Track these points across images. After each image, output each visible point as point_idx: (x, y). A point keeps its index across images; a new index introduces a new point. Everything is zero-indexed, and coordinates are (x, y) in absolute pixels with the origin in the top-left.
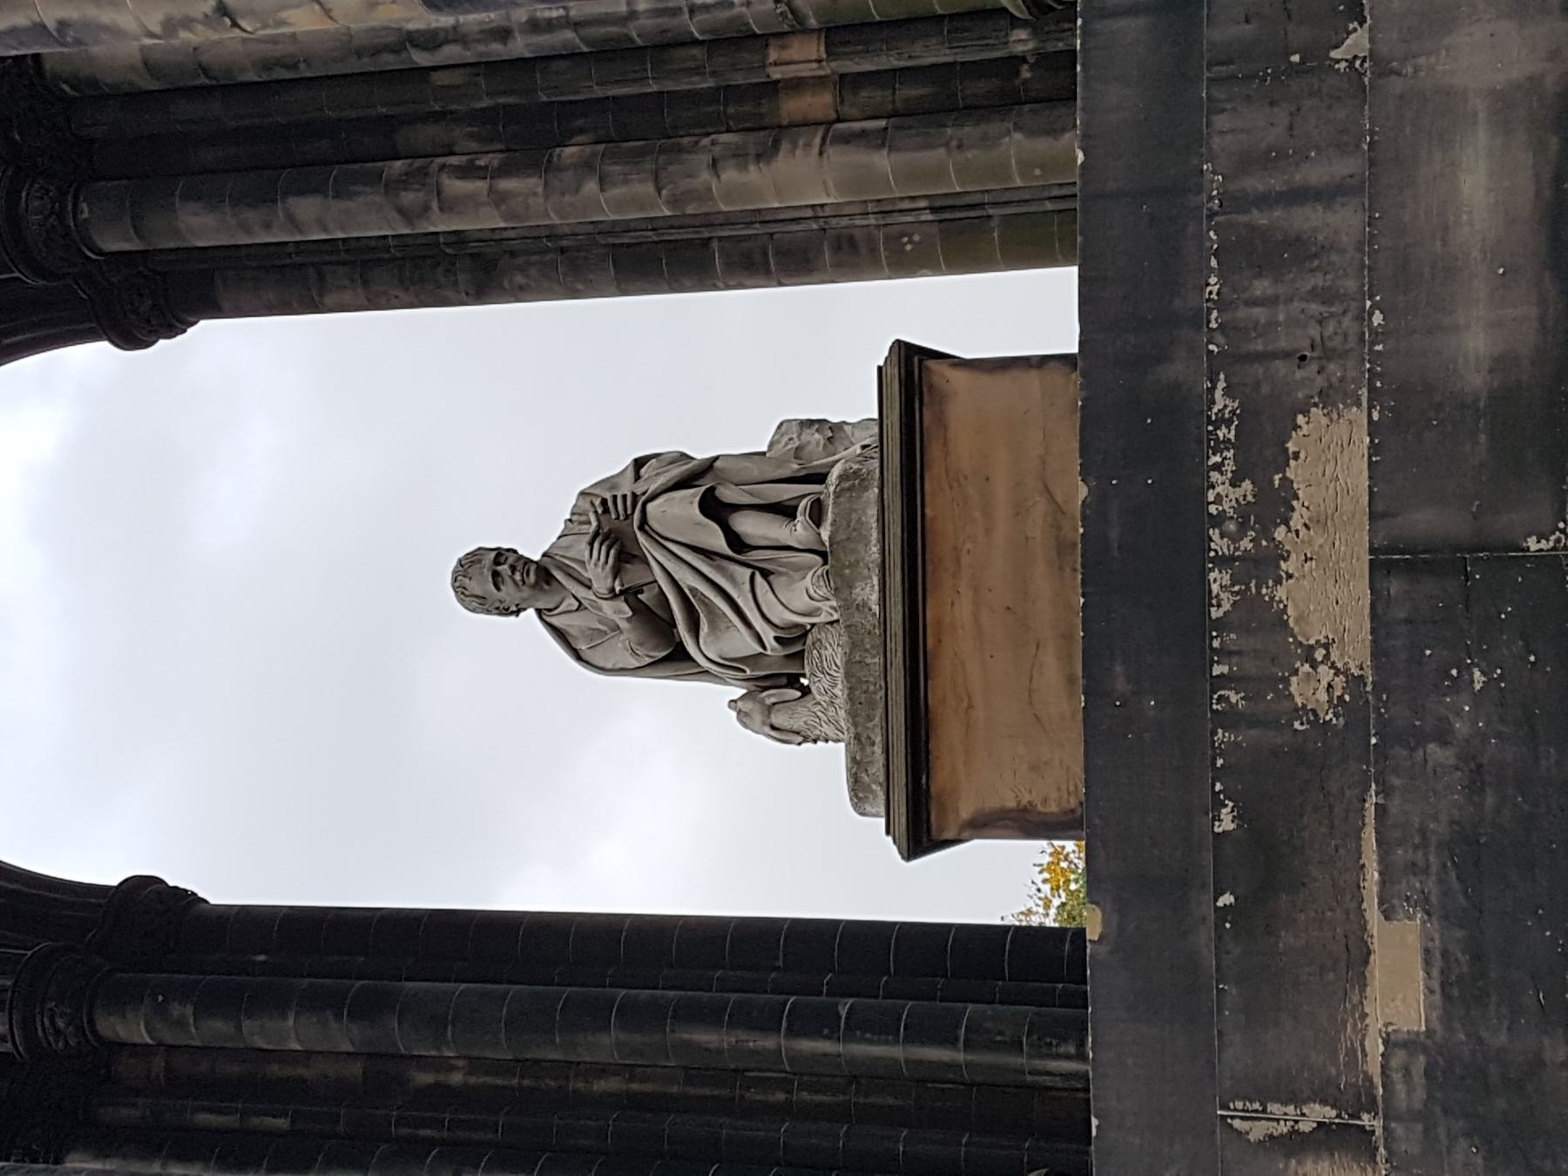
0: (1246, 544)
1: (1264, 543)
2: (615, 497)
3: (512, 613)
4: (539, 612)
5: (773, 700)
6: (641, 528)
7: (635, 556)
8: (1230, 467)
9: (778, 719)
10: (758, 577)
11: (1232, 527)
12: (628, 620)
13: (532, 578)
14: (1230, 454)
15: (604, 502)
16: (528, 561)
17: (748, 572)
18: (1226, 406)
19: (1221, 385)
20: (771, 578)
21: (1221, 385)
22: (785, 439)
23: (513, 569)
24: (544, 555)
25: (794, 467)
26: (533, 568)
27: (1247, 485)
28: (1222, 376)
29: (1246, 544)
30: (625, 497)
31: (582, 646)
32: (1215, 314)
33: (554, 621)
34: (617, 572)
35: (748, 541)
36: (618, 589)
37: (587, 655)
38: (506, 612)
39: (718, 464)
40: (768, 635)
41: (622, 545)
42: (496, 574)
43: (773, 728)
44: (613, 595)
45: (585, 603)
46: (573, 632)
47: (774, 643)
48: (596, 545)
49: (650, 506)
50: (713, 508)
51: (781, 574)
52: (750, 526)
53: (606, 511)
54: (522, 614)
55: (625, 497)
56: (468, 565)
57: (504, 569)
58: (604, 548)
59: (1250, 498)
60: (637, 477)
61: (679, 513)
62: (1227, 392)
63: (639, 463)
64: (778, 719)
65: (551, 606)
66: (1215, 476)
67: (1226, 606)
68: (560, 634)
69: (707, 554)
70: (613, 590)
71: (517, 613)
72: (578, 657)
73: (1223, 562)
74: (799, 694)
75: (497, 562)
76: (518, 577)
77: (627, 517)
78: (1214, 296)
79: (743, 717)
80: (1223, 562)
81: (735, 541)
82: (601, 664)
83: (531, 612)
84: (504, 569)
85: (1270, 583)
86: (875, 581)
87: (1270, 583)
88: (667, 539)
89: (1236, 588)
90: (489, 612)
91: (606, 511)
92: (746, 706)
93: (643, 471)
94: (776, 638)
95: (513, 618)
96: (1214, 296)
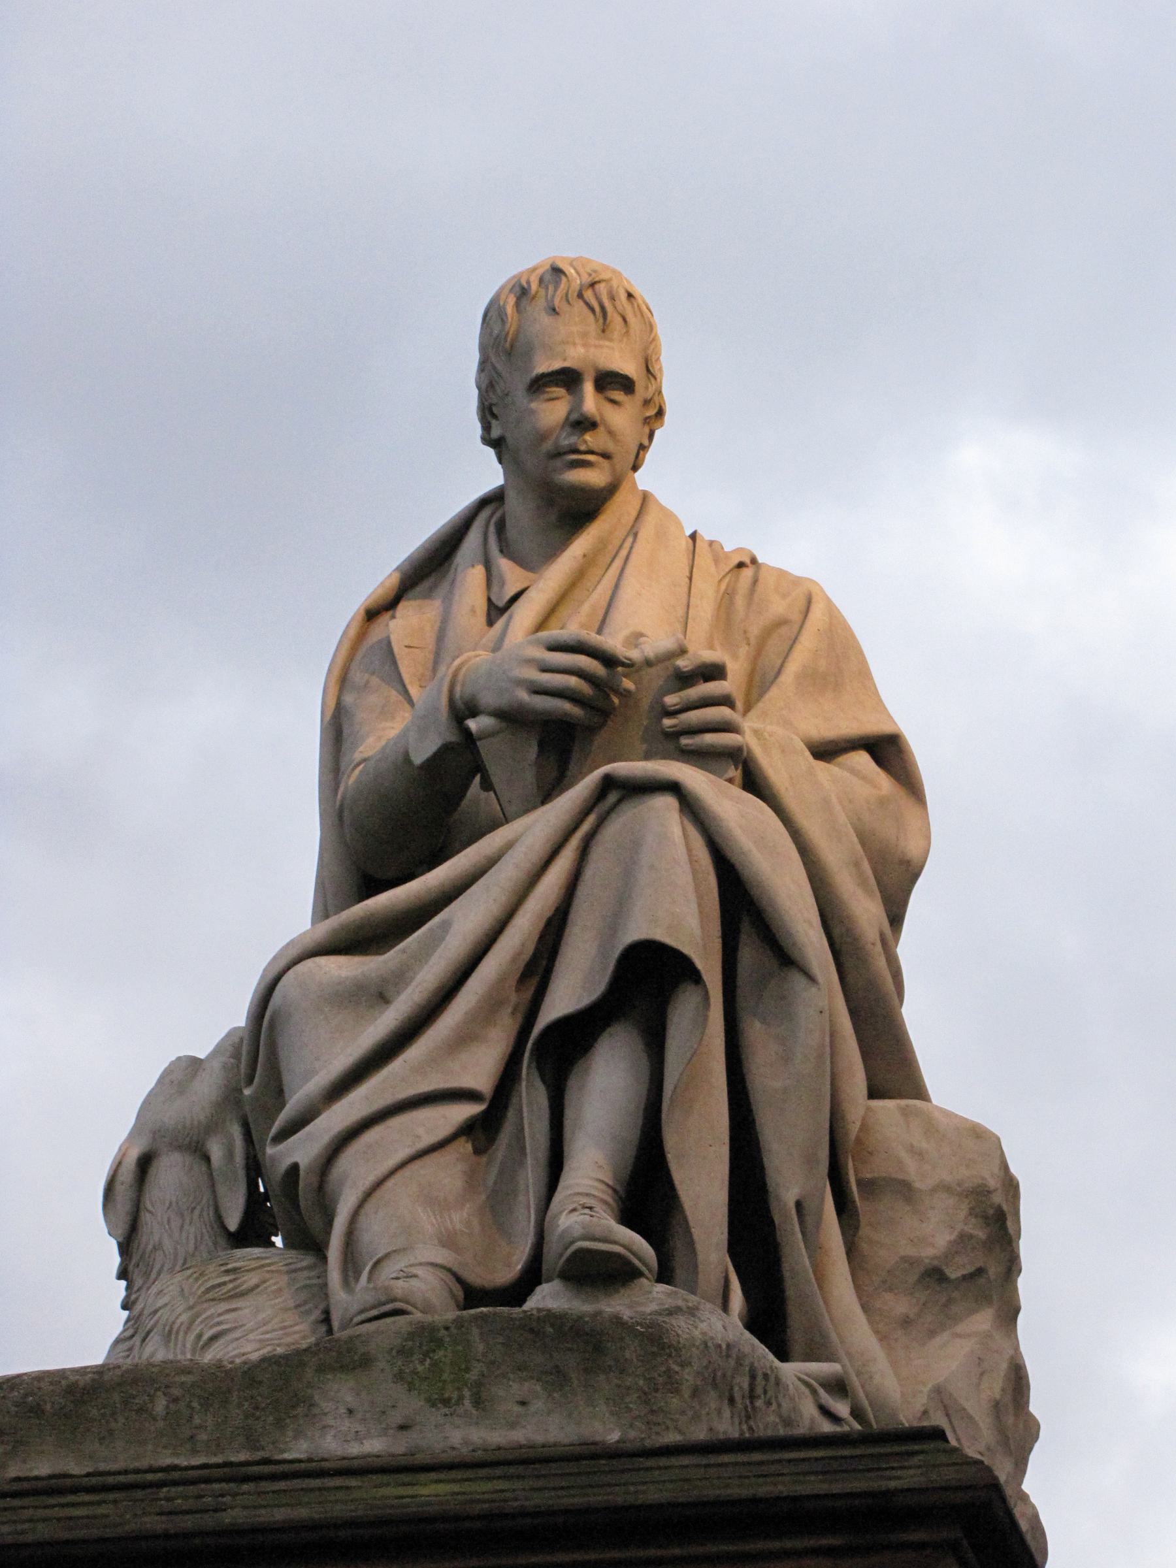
2: (726, 701)
3: (487, 427)
4: (493, 500)
5: (216, 1151)
6: (609, 783)
15: (714, 672)
20: (465, 1146)
30: (726, 727)
33: (473, 539)
34: (512, 718)
38: (487, 413)
39: (798, 980)
42: (569, 379)
43: (145, 1163)
47: (286, 1163)
48: (582, 661)
50: (647, 979)
52: (607, 1084)
53: (685, 679)
54: (490, 452)
55: (726, 727)
56: (604, 302)
57: (591, 401)
58: (573, 681)
63: (887, 750)
64: (171, 1173)
65: (511, 533)
69: (540, 966)
70: (474, 712)
74: (233, 1224)
75: (611, 382)
77: (675, 735)
86: (374, 1446)
91: (685, 679)
93: (862, 759)
94: (295, 1167)
95: (477, 429)
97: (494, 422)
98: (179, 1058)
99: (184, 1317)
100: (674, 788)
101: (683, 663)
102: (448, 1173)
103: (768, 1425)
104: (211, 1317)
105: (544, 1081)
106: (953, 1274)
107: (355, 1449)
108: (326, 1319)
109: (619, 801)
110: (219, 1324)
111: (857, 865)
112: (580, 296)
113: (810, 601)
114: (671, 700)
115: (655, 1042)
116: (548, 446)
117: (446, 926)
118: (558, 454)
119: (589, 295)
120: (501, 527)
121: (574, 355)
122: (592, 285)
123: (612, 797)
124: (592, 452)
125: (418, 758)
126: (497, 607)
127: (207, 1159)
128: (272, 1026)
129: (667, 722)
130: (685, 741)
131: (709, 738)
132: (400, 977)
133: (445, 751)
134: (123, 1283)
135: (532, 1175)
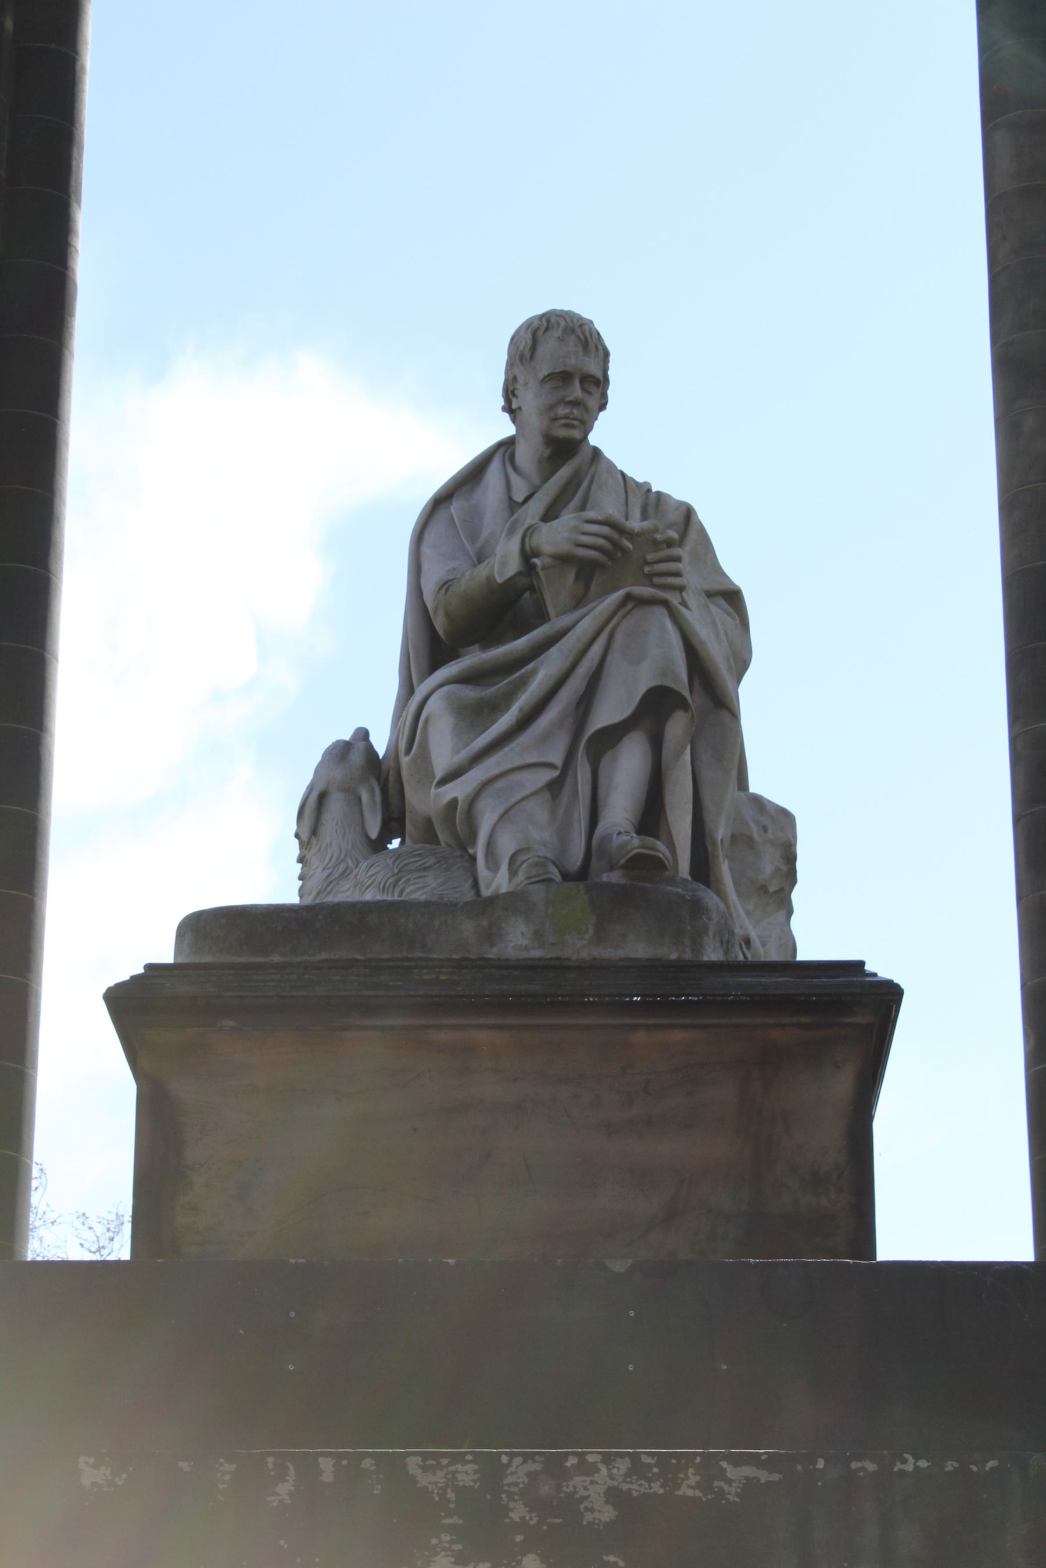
0: (518, 1512)
1: (519, 1538)
4: (506, 446)
5: (365, 796)
6: (629, 597)
7: (587, 588)
8: (637, 1488)
9: (336, 806)
10: (547, 776)
11: (545, 1489)
12: (490, 580)
13: (562, 433)
14: (657, 1488)
15: (669, 543)
16: (587, 426)
17: (556, 755)
18: (730, 1482)
19: (764, 1476)
20: (548, 796)
21: (764, 1476)
22: (765, 820)
23: (576, 403)
24: (596, 452)
25: (721, 832)
26: (576, 434)
27: (608, 1514)
28: (775, 1477)
29: (518, 1512)
30: (678, 574)
31: (456, 508)
32: (871, 1467)
33: (495, 466)
34: (563, 560)
35: (606, 760)
36: (537, 561)
37: (441, 516)
38: (510, 393)
39: (726, 716)
40: (459, 790)
41: (602, 566)
43: (322, 797)
44: (527, 555)
45: (520, 512)
46: (478, 493)
48: (606, 530)
49: (660, 614)
50: (656, 707)
51: (553, 812)
52: (629, 765)
53: (656, 544)
54: (506, 416)
55: (678, 574)
57: (576, 391)
58: (601, 542)
59: (589, 1517)
60: (710, 595)
61: (647, 660)
62: (750, 1483)
63: (733, 598)
64: (336, 806)
66: (623, 1466)
67: (424, 1480)
68: (473, 475)
70: (537, 555)
71: (509, 409)
72: (440, 501)
73: (493, 1472)
74: (374, 834)
76: (562, 411)
77: (650, 576)
78: (899, 1466)
79: (340, 752)
80: (493, 1472)
81: (610, 738)
82: (429, 537)
83: (508, 429)
84: (576, 391)
85: (457, 1547)
87: (457, 1547)
88: (611, 636)
89: (451, 1495)
90: (510, 366)
92: (357, 758)
93: (722, 602)
94: (455, 801)
95: (501, 402)
96: (899, 1466)
97: (514, 400)
98: (338, 742)
99: (392, 879)
100: (665, 603)
101: (659, 537)
102: (539, 810)
103: (731, 958)
104: (409, 880)
105: (589, 761)
106: (772, 889)
107: (525, 955)
108: (476, 885)
109: (633, 608)
110: (415, 884)
111: (728, 659)
112: (573, 331)
113: (688, 514)
114: (650, 557)
115: (656, 743)
116: (552, 415)
117: (533, 673)
118: (555, 419)
119: (579, 331)
120: (512, 458)
121: (572, 363)
122: (581, 326)
123: (629, 606)
124: (575, 419)
125: (500, 580)
126: (515, 502)
127: (360, 799)
128: (427, 721)
129: (647, 569)
130: (656, 580)
131: (671, 580)
132: (508, 698)
133: (519, 574)
134: (300, 865)
135: (582, 813)
